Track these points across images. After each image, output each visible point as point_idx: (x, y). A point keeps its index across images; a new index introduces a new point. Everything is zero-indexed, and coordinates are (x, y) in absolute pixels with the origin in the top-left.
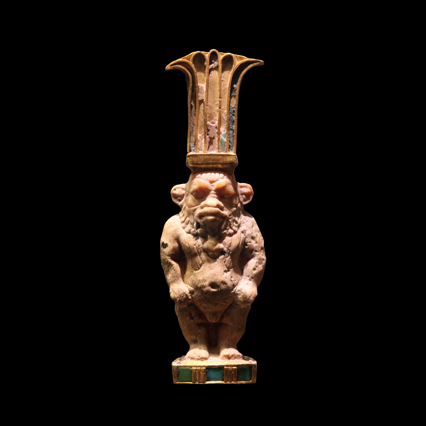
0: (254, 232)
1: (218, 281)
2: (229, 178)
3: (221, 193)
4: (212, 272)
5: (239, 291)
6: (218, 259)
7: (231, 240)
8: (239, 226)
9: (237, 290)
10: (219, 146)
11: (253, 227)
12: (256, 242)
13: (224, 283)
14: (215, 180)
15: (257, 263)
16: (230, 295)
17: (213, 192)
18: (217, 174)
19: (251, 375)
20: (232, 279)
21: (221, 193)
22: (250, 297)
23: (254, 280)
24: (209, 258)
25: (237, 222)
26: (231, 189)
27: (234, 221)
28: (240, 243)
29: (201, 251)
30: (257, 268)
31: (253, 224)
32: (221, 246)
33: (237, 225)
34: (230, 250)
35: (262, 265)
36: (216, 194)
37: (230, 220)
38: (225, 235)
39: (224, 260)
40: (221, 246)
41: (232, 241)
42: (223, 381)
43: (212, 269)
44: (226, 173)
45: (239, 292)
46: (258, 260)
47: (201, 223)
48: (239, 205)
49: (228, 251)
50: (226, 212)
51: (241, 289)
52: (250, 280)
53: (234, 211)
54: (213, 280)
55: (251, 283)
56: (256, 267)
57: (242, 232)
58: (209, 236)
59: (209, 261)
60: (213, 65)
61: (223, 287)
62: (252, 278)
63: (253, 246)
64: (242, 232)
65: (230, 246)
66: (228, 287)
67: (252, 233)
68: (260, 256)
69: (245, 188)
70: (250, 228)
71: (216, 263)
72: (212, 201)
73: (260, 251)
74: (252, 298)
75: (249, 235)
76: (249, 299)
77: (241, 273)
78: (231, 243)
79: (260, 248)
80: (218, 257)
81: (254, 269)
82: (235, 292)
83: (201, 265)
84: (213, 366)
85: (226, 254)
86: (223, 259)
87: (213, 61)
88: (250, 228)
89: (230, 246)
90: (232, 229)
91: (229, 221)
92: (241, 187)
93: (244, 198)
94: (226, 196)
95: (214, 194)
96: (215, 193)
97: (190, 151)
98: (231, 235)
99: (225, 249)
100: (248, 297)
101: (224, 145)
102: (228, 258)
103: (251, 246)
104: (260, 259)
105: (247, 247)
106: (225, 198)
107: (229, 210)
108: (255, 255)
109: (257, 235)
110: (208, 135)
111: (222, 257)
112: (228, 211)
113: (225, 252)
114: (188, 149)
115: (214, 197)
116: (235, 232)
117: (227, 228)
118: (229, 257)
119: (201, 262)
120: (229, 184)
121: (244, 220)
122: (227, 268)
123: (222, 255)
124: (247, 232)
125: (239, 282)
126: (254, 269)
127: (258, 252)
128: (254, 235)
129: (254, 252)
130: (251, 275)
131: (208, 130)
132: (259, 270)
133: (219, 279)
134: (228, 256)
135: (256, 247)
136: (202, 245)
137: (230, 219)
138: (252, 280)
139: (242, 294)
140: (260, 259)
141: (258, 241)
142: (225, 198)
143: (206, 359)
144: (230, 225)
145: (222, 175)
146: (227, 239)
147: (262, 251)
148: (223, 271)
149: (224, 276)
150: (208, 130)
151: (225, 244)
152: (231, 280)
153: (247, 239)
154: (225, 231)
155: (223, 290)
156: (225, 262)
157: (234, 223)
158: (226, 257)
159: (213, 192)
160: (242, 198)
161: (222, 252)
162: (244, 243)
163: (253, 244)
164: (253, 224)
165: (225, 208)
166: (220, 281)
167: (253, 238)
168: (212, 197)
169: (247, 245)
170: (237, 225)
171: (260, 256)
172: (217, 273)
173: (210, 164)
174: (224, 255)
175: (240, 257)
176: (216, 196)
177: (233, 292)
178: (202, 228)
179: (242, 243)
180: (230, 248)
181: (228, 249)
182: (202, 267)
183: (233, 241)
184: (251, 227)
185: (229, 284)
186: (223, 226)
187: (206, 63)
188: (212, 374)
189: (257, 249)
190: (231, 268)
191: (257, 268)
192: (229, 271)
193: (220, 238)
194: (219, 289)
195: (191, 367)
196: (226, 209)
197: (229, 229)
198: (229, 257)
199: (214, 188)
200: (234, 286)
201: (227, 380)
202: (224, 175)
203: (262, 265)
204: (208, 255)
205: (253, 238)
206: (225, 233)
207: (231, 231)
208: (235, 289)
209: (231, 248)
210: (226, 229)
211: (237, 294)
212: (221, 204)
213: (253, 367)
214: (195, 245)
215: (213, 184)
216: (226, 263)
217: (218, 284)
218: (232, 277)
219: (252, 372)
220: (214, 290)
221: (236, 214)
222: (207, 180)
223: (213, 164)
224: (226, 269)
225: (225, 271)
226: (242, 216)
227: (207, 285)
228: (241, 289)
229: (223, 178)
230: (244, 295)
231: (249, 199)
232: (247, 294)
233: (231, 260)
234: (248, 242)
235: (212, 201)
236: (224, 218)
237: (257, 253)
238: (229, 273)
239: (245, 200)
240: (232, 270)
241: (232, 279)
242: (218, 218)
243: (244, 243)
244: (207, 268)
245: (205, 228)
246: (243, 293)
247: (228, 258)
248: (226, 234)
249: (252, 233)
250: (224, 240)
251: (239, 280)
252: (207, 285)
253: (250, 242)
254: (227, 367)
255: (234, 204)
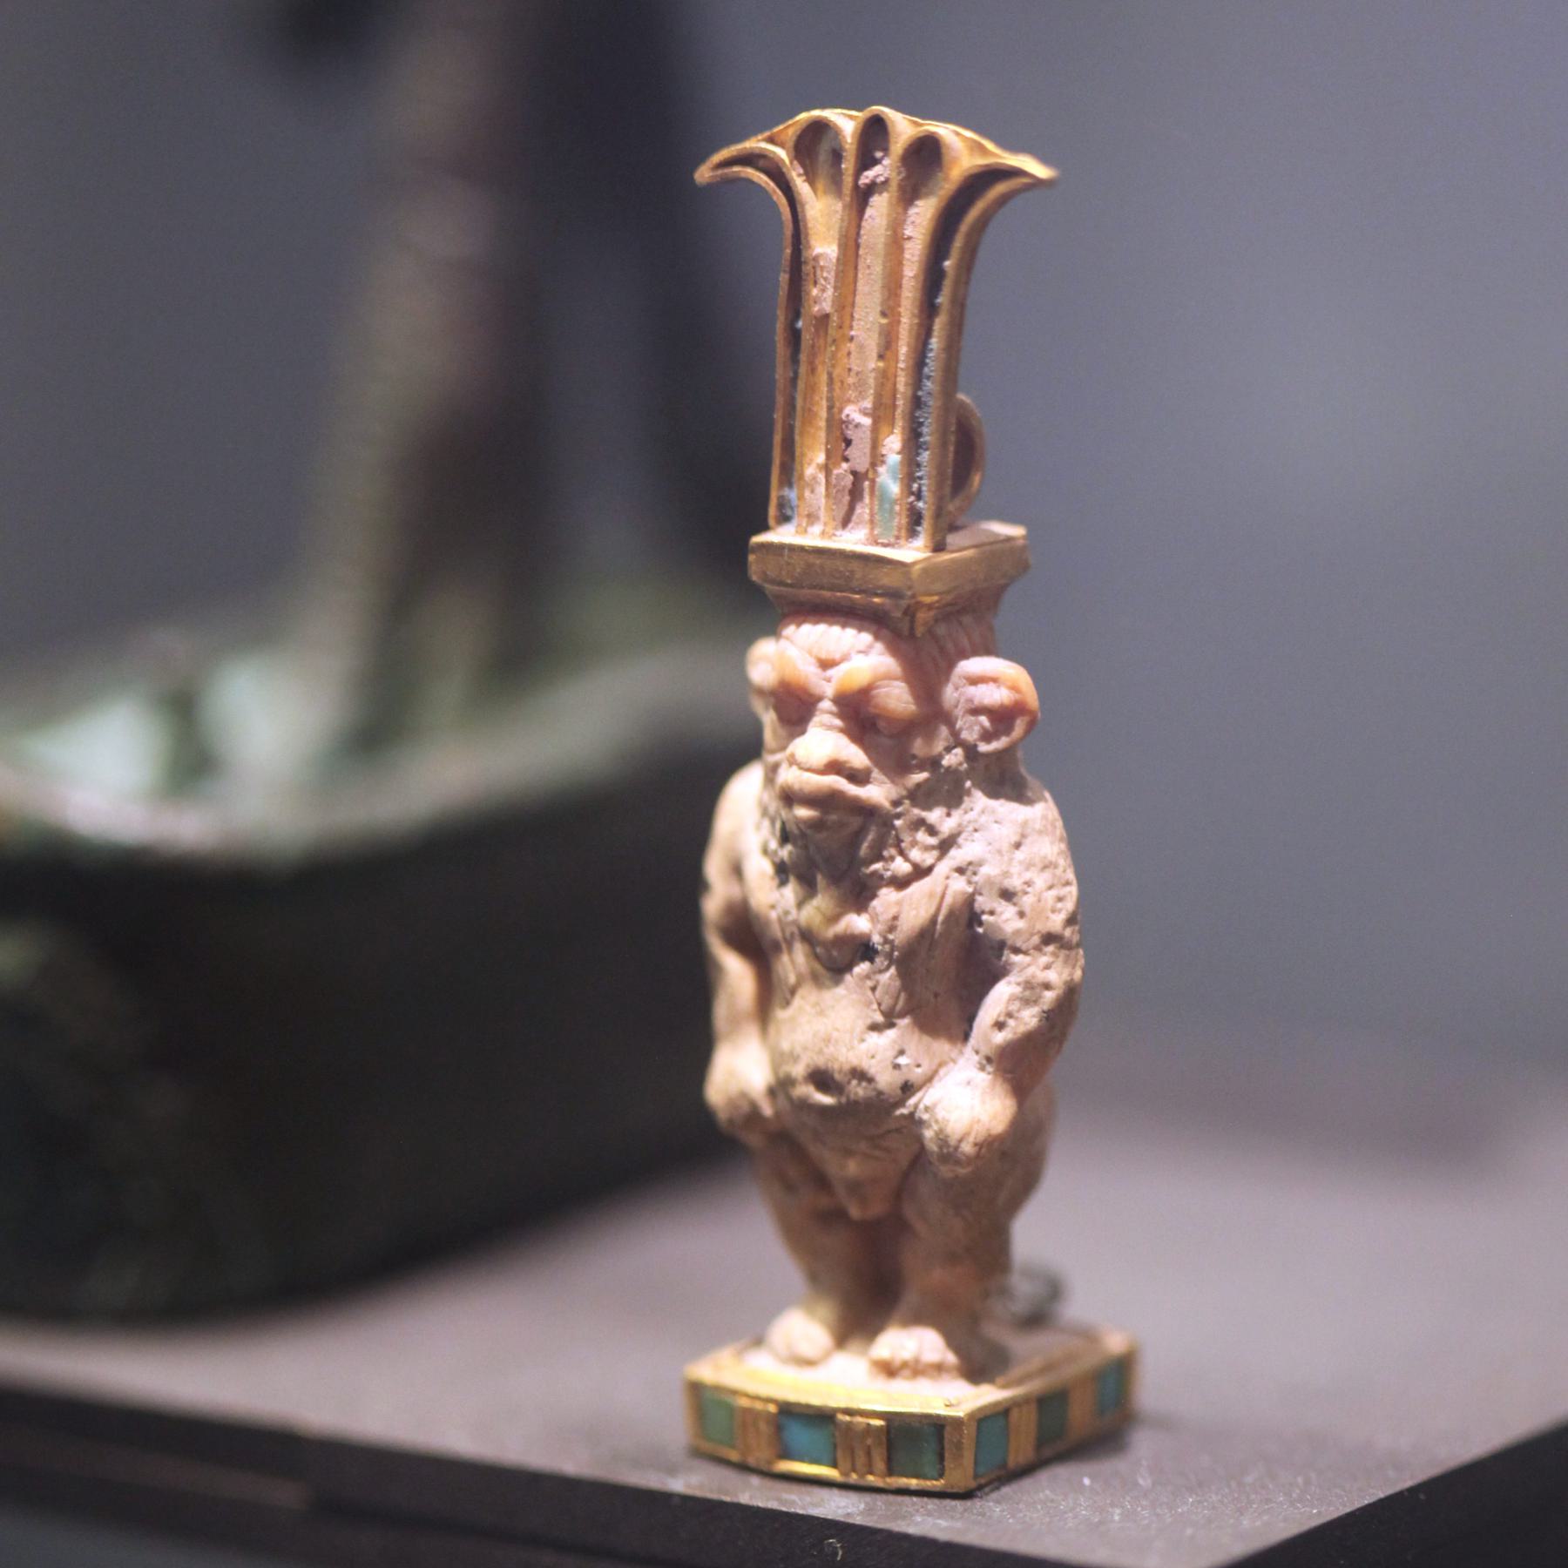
0: (1015, 870)
1: (836, 1066)
2: (894, 650)
3: (858, 714)
4: (821, 1026)
5: (927, 1109)
6: (848, 977)
7: (899, 903)
8: (946, 846)
9: (921, 1106)
10: (872, 515)
11: (1018, 846)
12: (1021, 914)
13: (860, 1075)
14: (837, 656)
15: (1012, 998)
16: (892, 1125)
17: (826, 705)
18: (850, 633)
19: (941, 1458)
20: (902, 1060)
21: (858, 714)
22: (960, 1141)
23: (995, 1073)
24: (818, 967)
25: (932, 831)
26: (898, 698)
27: (920, 823)
28: (941, 918)
29: (792, 934)
30: (1011, 1022)
31: (1023, 836)
32: (859, 923)
33: (933, 841)
34: (891, 942)
35: (1035, 1010)
36: (840, 715)
37: (898, 823)
38: (879, 881)
39: (869, 983)
40: (859, 923)
41: (903, 909)
42: (834, 1465)
43: (822, 1013)
44: (885, 632)
45: (925, 1117)
46: (1018, 990)
47: (792, 827)
48: (954, 758)
49: (887, 947)
50: (877, 792)
51: (935, 1105)
52: (982, 1068)
53: (919, 785)
54: (820, 1062)
55: (983, 1078)
56: (1010, 1015)
57: (960, 871)
58: (819, 878)
59: (816, 980)
60: (877, 170)
61: (858, 1090)
62: (989, 1059)
63: (1000, 929)
64: (960, 871)
65: (892, 929)
66: (880, 1093)
67: (1006, 874)
68: (1031, 971)
69: (992, 686)
70: (999, 852)
71: (840, 991)
72: (823, 741)
73: (1038, 948)
74: (967, 1148)
75: (989, 881)
76: (957, 1148)
77: (961, 1030)
78: (895, 918)
79: (1036, 940)
80: (848, 968)
81: (1000, 1026)
82: (912, 1115)
83: (793, 992)
84: (798, 1405)
85: (878, 960)
86: (868, 977)
87: (879, 154)
88: (999, 852)
89: (892, 929)
90: (907, 859)
91: (893, 827)
92: (975, 681)
93: (983, 727)
94: (881, 724)
95: (831, 713)
96: (834, 709)
97: (785, 519)
98: (901, 883)
99: (876, 939)
100: (953, 1142)
101: (891, 510)
102: (887, 975)
103: (995, 927)
104: (1028, 985)
105: (980, 930)
106: (878, 732)
107: (893, 782)
108: (1012, 964)
109: (1028, 883)
110: (846, 460)
111: (863, 968)
112: (889, 785)
113: (876, 952)
114: (772, 511)
115: (830, 727)
116: (921, 872)
117: (885, 853)
118: (893, 970)
119: (792, 979)
120: (889, 677)
121: (983, 819)
122: (883, 1013)
123: (863, 959)
124: (985, 870)
125: (942, 1072)
126: (1000, 1026)
127: (1025, 953)
128: (1015, 883)
129: (1006, 952)
130: (985, 1050)
131: (848, 443)
132: (1022, 1029)
133: (842, 1059)
134: (888, 968)
135: (1017, 932)
136: (794, 911)
137: (898, 816)
138: (989, 1068)
139: (936, 1127)
140: (1028, 985)
141: (1027, 910)
142: (878, 732)
143: (808, 1363)
144: (899, 841)
145: (866, 638)
146: (887, 898)
147: (1051, 948)
148: (861, 1025)
149: (864, 1046)
150: (848, 443)
151: (874, 919)
152: (897, 1067)
153: (979, 899)
154: (877, 866)
155: (856, 1103)
156: (873, 989)
157: (922, 836)
158: (881, 972)
159: (826, 705)
160: (971, 729)
161: (862, 949)
162: (968, 914)
163: (1005, 920)
164: (1023, 836)
165: (876, 774)
166: (846, 1067)
167: (1007, 895)
168: (823, 725)
169: (981, 924)
170: (933, 841)
171: (1031, 971)
172: (835, 1034)
173: (822, 588)
174: (872, 960)
175: (947, 972)
176: (838, 722)
177: (904, 1111)
178: (795, 845)
179: (951, 914)
180: (891, 937)
181: (886, 941)
182: (797, 1001)
183: (906, 907)
184: (1005, 846)
185: (886, 1080)
186: (865, 845)
187: (848, 165)
188: (798, 1435)
189: (1019, 944)
190: (902, 1015)
191: (1011, 1022)
192: (891, 1025)
193: (860, 894)
194: (844, 1100)
195: (735, 1392)
196: (883, 778)
197: (892, 859)
198: (893, 970)
199: (829, 690)
200: (908, 1089)
201: (849, 1465)
202: (877, 637)
203: (1035, 1010)
204: (817, 957)
205: (1007, 895)
206: (875, 873)
207: (901, 866)
208: (912, 1101)
209: (898, 937)
210: (879, 857)
211: (921, 1122)
212: (856, 756)
213: (948, 1429)
214: (773, 907)
215: (832, 672)
216: (878, 992)
217: (837, 1076)
218: (902, 1052)
219: (947, 1446)
220: (826, 1100)
221: (947, 791)
222: (810, 653)
223: (832, 588)
224: (879, 1018)
225: (875, 1027)
226: (979, 801)
227: (800, 1078)
228: (935, 1105)
229: (864, 652)
230: (941, 1130)
231: (1008, 730)
232: (949, 1130)
233: (898, 983)
234: (983, 912)
235: (823, 741)
236: (868, 812)
237: (1018, 959)
238: (891, 1034)
239: (987, 736)
240: (905, 1022)
241: (902, 1060)
242: (833, 817)
243: (968, 914)
244: (808, 1008)
245: (806, 847)
246: (937, 1121)
247: (888, 977)
248: (881, 877)
249: (1006, 874)
250: (875, 903)
251: (941, 1065)
252: (800, 1078)
253: (992, 913)
254: (848, 1418)
255: (914, 757)
